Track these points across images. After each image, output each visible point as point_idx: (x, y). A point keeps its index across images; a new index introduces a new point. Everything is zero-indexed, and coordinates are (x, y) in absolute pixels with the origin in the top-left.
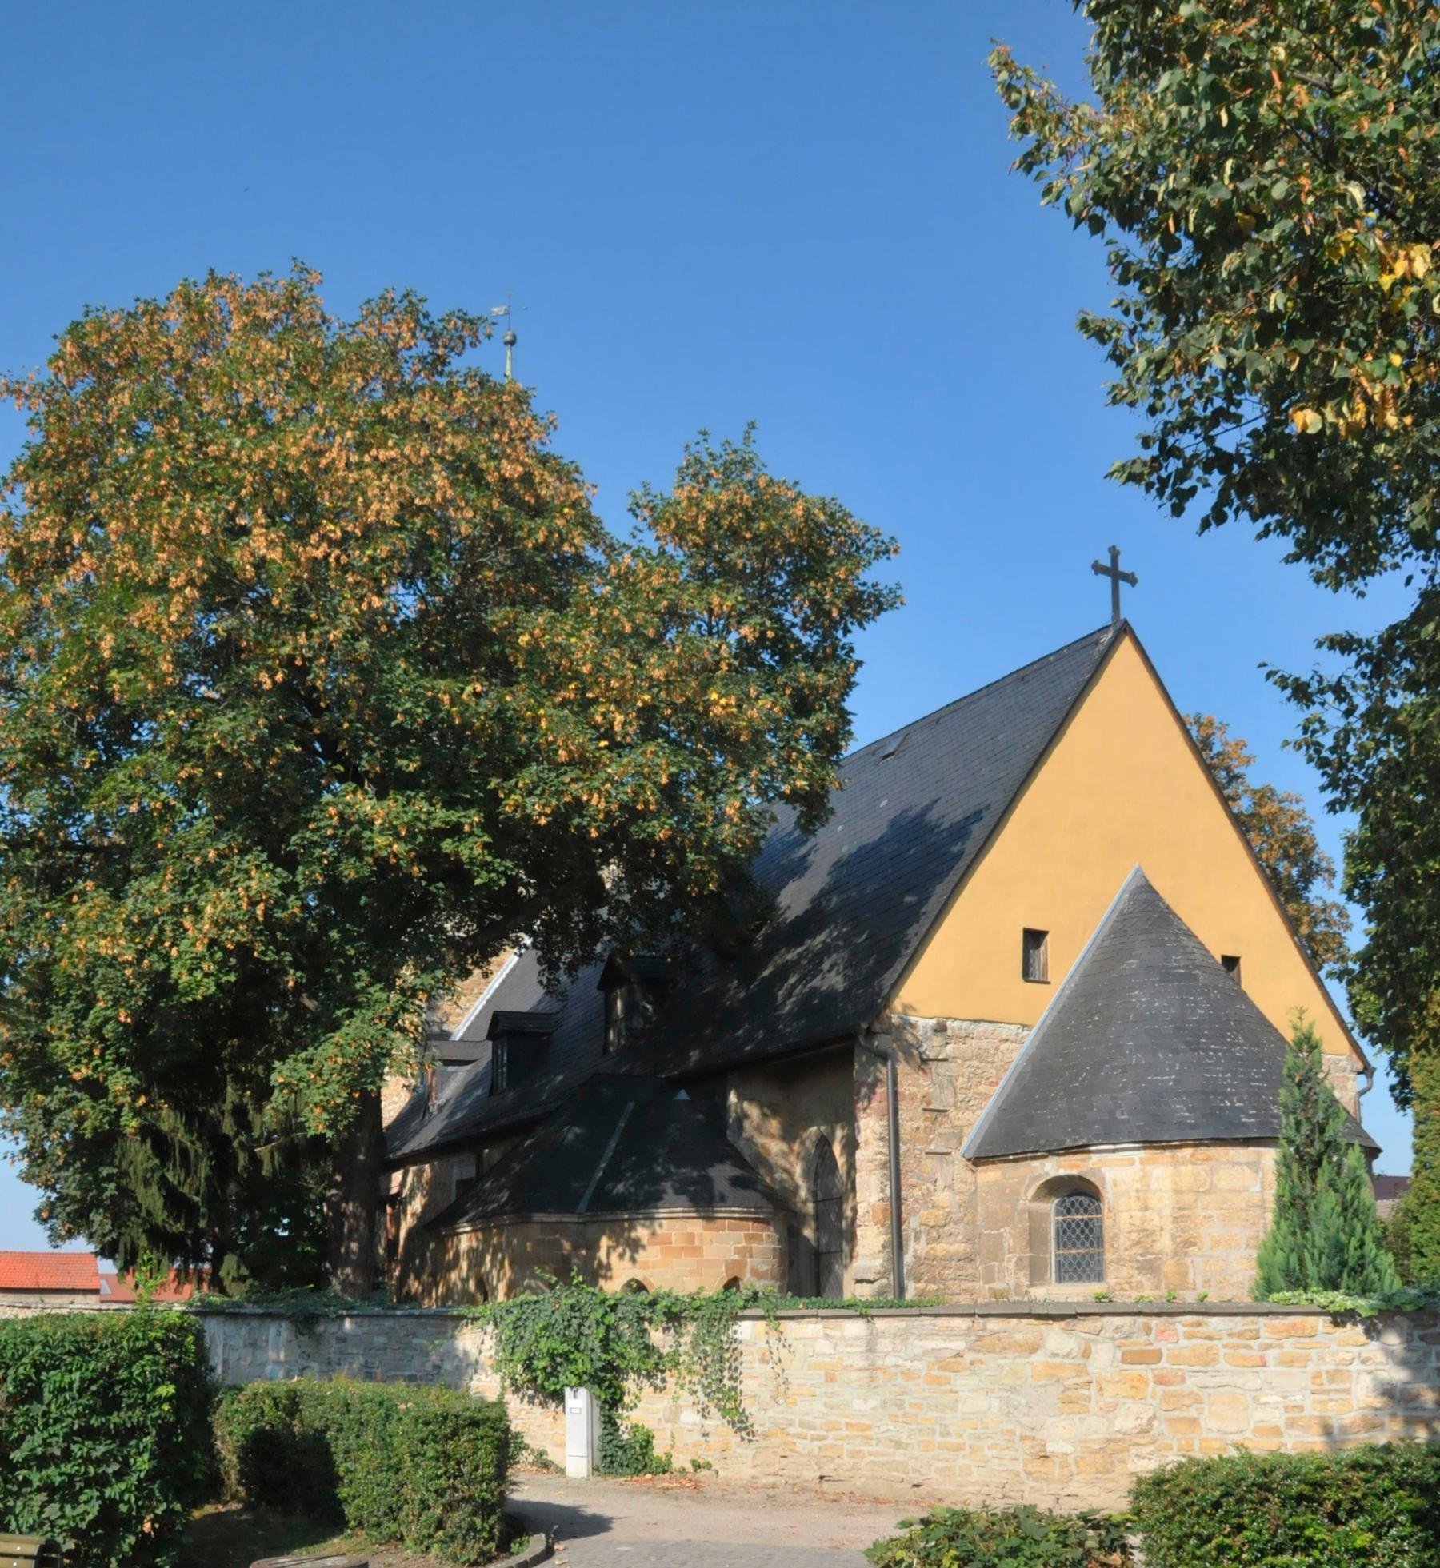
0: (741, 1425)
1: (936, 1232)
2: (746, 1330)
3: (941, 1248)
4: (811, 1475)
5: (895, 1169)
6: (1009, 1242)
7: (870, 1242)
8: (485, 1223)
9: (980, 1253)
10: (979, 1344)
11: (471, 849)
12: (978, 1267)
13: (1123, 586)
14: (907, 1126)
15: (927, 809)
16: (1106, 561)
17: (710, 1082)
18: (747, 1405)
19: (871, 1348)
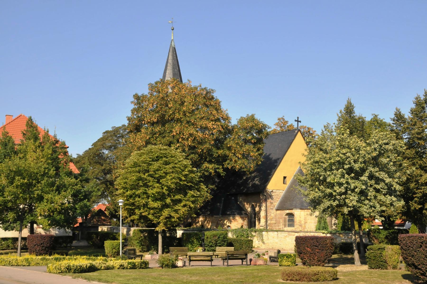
0: (264, 243)
1: (271, 220)
2: (264, 233)
3: (272, 222)
4: (271, 248)
5: (266, 211)
6: (281, 221)
7: (263, 221)
8: (205, 216)
9: (278, 223)
10: (289, 235)
11: (221, 171)
12: (277, 225)
13: (299, 123)
14: (268, 205)
15: (269, 155)
16: (297, 120)
17: (236, 195)
18: (264, 241)
19: (278, 235)
